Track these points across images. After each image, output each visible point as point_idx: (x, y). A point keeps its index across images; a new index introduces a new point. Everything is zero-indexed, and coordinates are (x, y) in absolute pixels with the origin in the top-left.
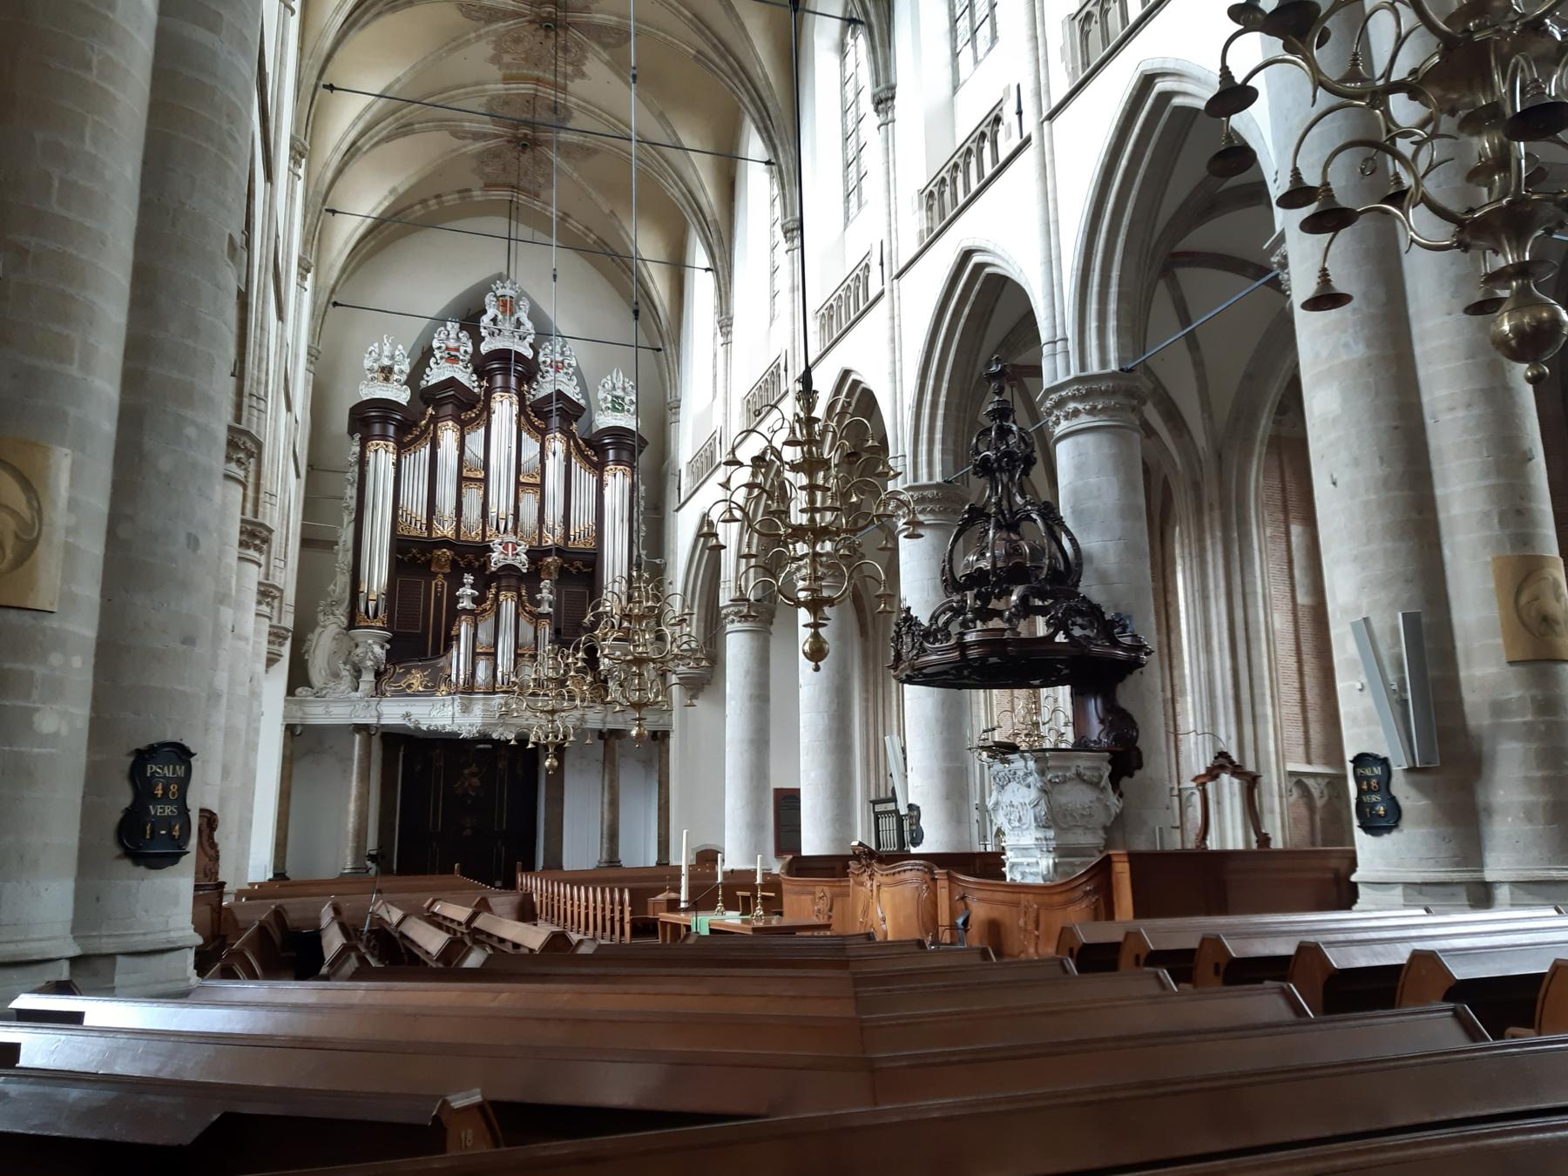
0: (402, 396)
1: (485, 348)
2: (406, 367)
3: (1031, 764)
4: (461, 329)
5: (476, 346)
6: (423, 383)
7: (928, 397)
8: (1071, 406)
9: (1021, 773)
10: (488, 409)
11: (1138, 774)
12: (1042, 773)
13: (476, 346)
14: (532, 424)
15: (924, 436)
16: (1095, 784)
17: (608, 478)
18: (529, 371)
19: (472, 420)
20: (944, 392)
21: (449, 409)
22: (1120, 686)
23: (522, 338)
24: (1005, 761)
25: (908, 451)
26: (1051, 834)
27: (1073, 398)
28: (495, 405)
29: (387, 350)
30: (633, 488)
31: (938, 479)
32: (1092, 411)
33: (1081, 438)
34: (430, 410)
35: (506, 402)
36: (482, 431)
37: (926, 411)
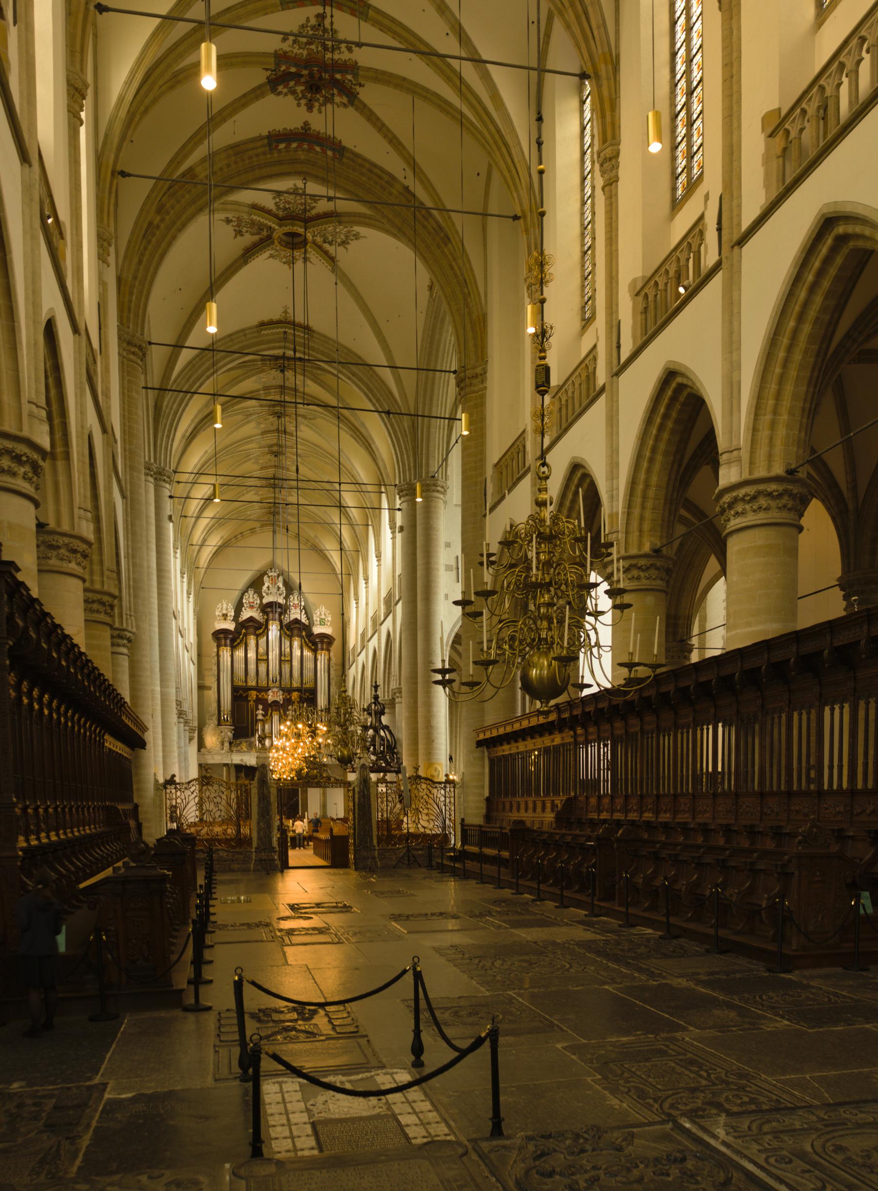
0: (231, 626)
1: (265, 601)
2: (233, 614)
4: (255, 593)
5: (261, 601)
6: (240, 620)
10: (267, 628)
13: (261, 601)
14: (286, 633)
17: (319, 657)
18: (284, 609)
19: (260, 634)
21: (251, 630)
23: (280, 595)
28: (270, 627)
29: (225, 606)
30: (329, 660)
34: (244, 631)
35: (274, 626)
36: (265, 638)
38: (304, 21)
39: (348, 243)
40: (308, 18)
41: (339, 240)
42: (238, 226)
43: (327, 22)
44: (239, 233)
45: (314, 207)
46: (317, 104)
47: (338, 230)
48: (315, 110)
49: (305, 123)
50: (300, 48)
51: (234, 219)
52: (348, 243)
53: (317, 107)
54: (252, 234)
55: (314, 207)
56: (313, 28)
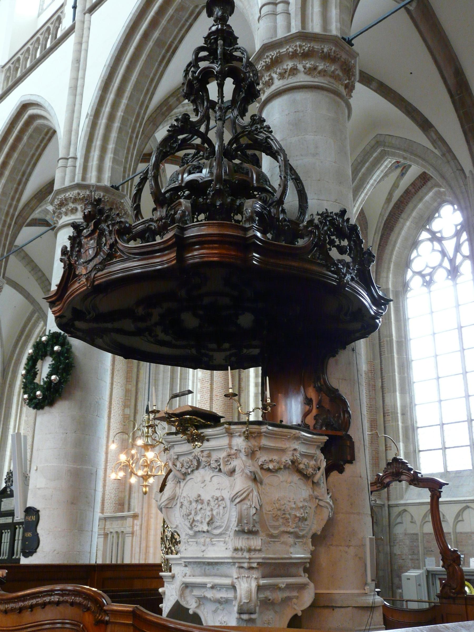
3: (239, 442)
7: (107, 109)
8: (289, 65)
9: (223, 455)
11: (348, 467)
12: (251, 454)
15: (98, 143)
16: (306, 477)
20: (122, 106)
22: (332, 361)
24: (192, 439)
25: (80, 154)
26: (256, 542)
27: (294, 56)
31: (106, 182)
32: (310, 71)
33: (299, 96)
37: (103, 121)
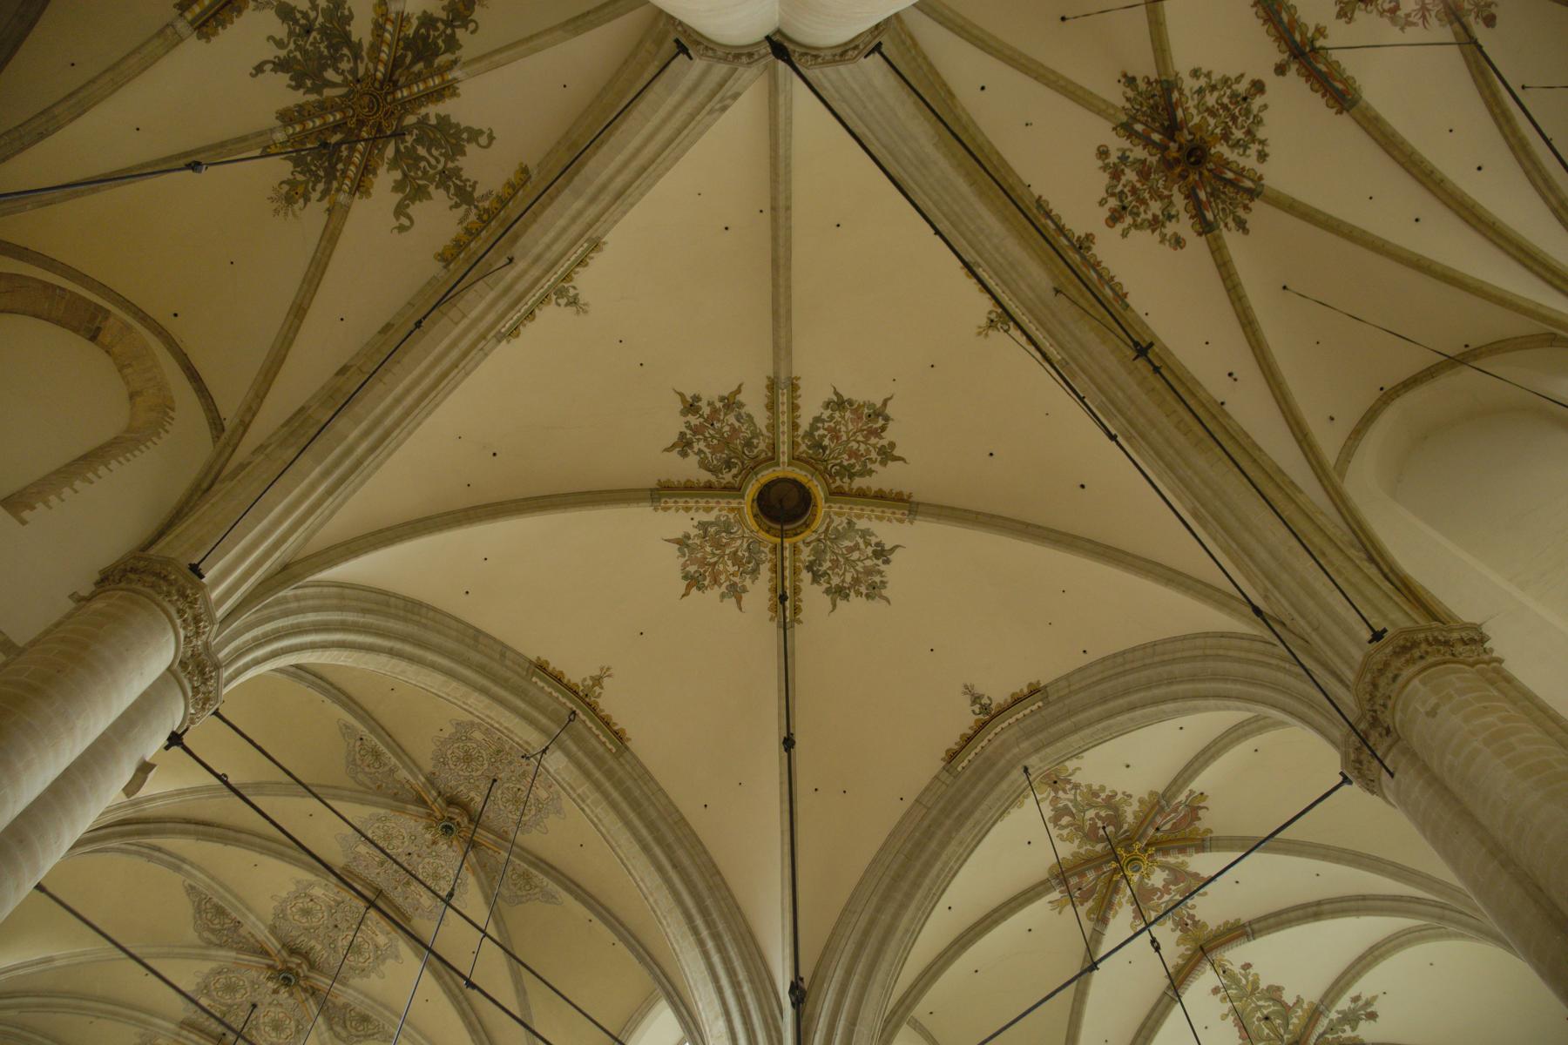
38: (1233, 75)
39: (846, 597)
40: (1242, 75)
41: (835, 581)
42: (696, 430)
43: (1257, 102)
44: (683, 445)
45: (870, 472)
46: (1129, 220)
47: (855, 555)
48: (1119, 227)
49: (1088, 236)
50: (1197, 107)
51: (706, 411)
52: (846, 597)
53: (1125, 225)
54: (703, 464)
55: (870, 472)
56: (1234, 95)
